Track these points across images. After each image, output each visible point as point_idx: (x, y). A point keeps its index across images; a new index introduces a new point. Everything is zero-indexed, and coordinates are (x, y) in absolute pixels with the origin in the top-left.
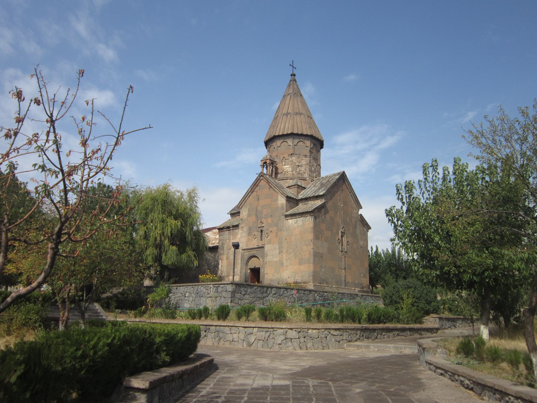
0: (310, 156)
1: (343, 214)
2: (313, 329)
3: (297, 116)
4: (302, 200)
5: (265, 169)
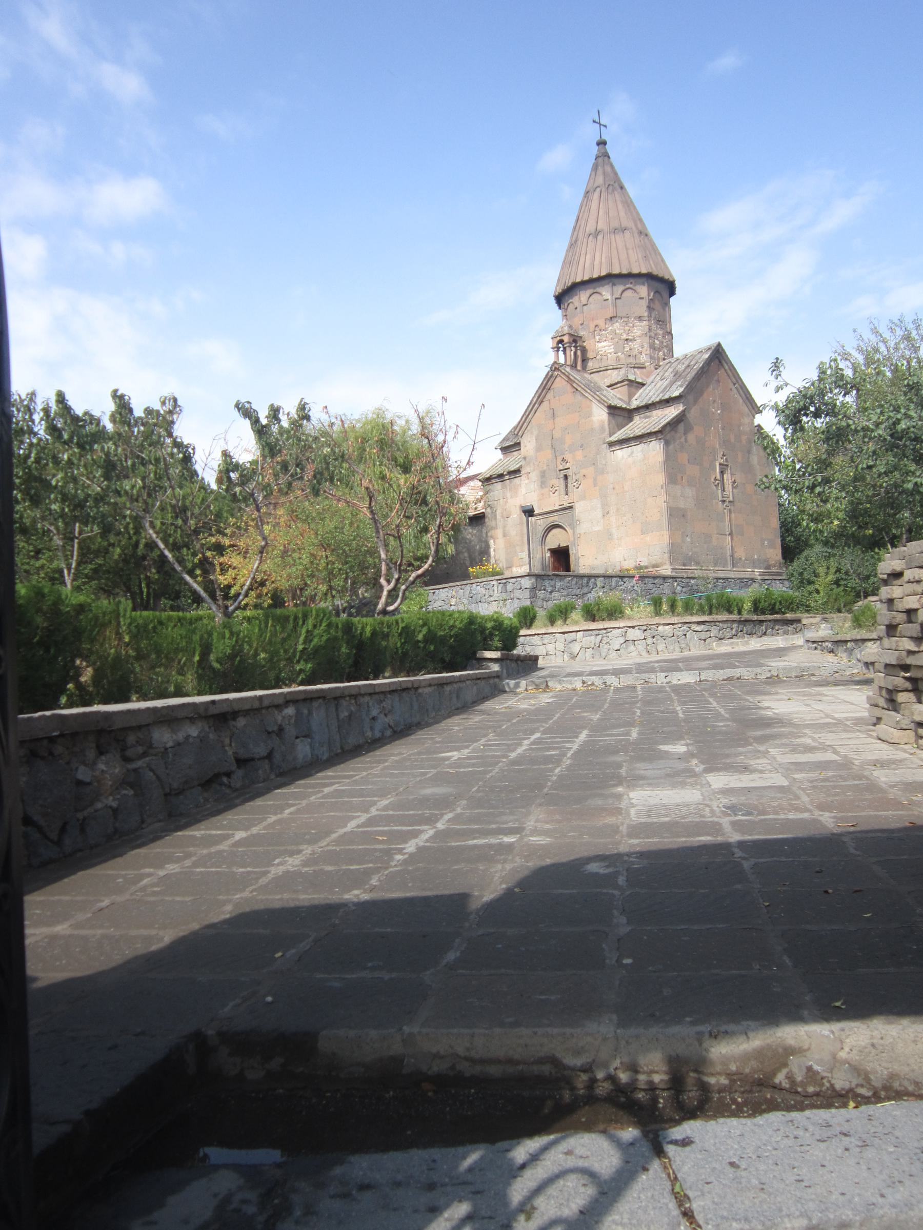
0: (650, 316)
1: (723, 429)
2: (664, 624)
3: (617, 236)
4: (638, 409)
5: (561, 353)
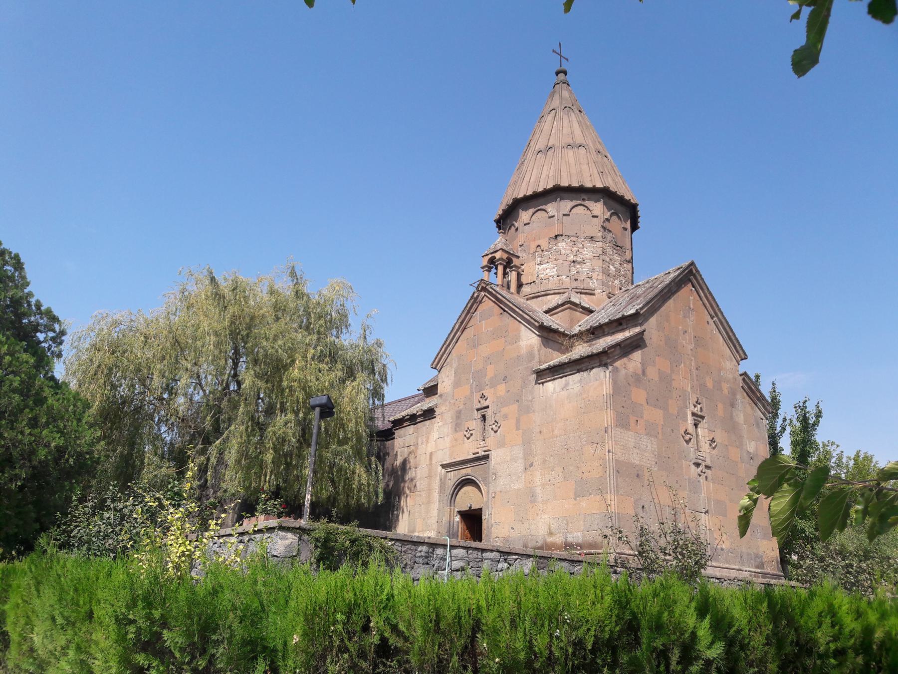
1: (697, 369)
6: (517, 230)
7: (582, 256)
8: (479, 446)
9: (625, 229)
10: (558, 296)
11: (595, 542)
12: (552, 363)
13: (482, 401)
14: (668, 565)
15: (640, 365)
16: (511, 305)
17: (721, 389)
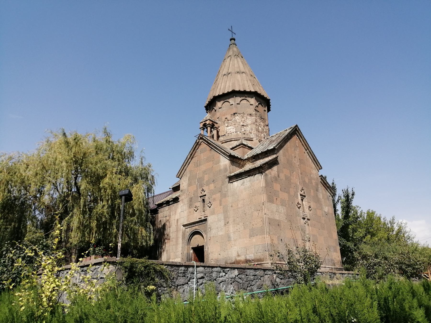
1: (301, 174)
6: (216, 111)
7: (246, 123)
8: (202, 215)
9: (265, 111)
10: (236, 141)
11: (260, 258)
12: (236, 173)
13: (203, 192)
14: (301, 267)
15: (277, 173)
16: (215, 146)
17: (312, 183)
